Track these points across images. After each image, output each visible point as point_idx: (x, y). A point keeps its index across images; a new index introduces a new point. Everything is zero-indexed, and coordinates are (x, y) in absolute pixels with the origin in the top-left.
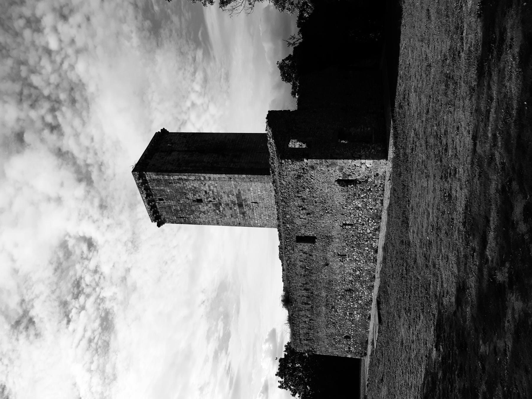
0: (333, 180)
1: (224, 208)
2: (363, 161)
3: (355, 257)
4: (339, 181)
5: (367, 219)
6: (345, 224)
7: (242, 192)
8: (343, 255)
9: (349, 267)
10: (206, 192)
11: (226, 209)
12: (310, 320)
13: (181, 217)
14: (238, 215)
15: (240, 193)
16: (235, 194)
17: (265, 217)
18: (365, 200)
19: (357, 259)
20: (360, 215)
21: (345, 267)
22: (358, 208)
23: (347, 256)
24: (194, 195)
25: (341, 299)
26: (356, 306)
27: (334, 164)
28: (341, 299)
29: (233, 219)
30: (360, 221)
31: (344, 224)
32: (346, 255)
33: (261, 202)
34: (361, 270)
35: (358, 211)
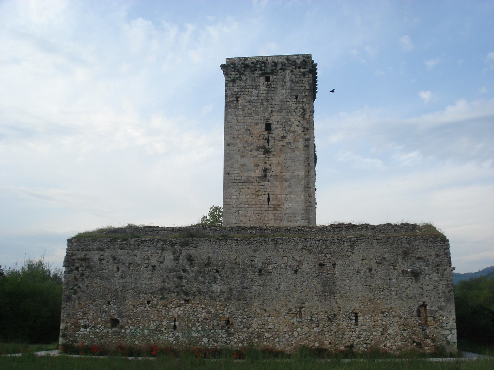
0: (426, 300)
1: (256, 157)
2: (455, 332)
3: (299, 330)
4: (424, 305)
5: (368, 342)
6: (357, 317)
7: (287, 183)
8: (300, 315)
9: (278, 322)
10: (284, 137)
11: (256, 159)
12: (154, 267)
13: (237, 98)
14: (246, 174)
15: (285, 180)
16: (282, 174)
17: (243, 209)
18: (399, 337)
19: (295, 334)
20: (374, 333)
21: (277, 317)
22: (385, 330)
23: (300, 320)
24: (278, 122)
25: (208, 313)
26: (194, 335)
27: (448, 300)
28: (208, 313)
29: (237, 166)
30: (364, 333)
31: (356, 314)
32: (301, 318)
33: (271, 206)
34: (274, 339)
35: (381, 330)
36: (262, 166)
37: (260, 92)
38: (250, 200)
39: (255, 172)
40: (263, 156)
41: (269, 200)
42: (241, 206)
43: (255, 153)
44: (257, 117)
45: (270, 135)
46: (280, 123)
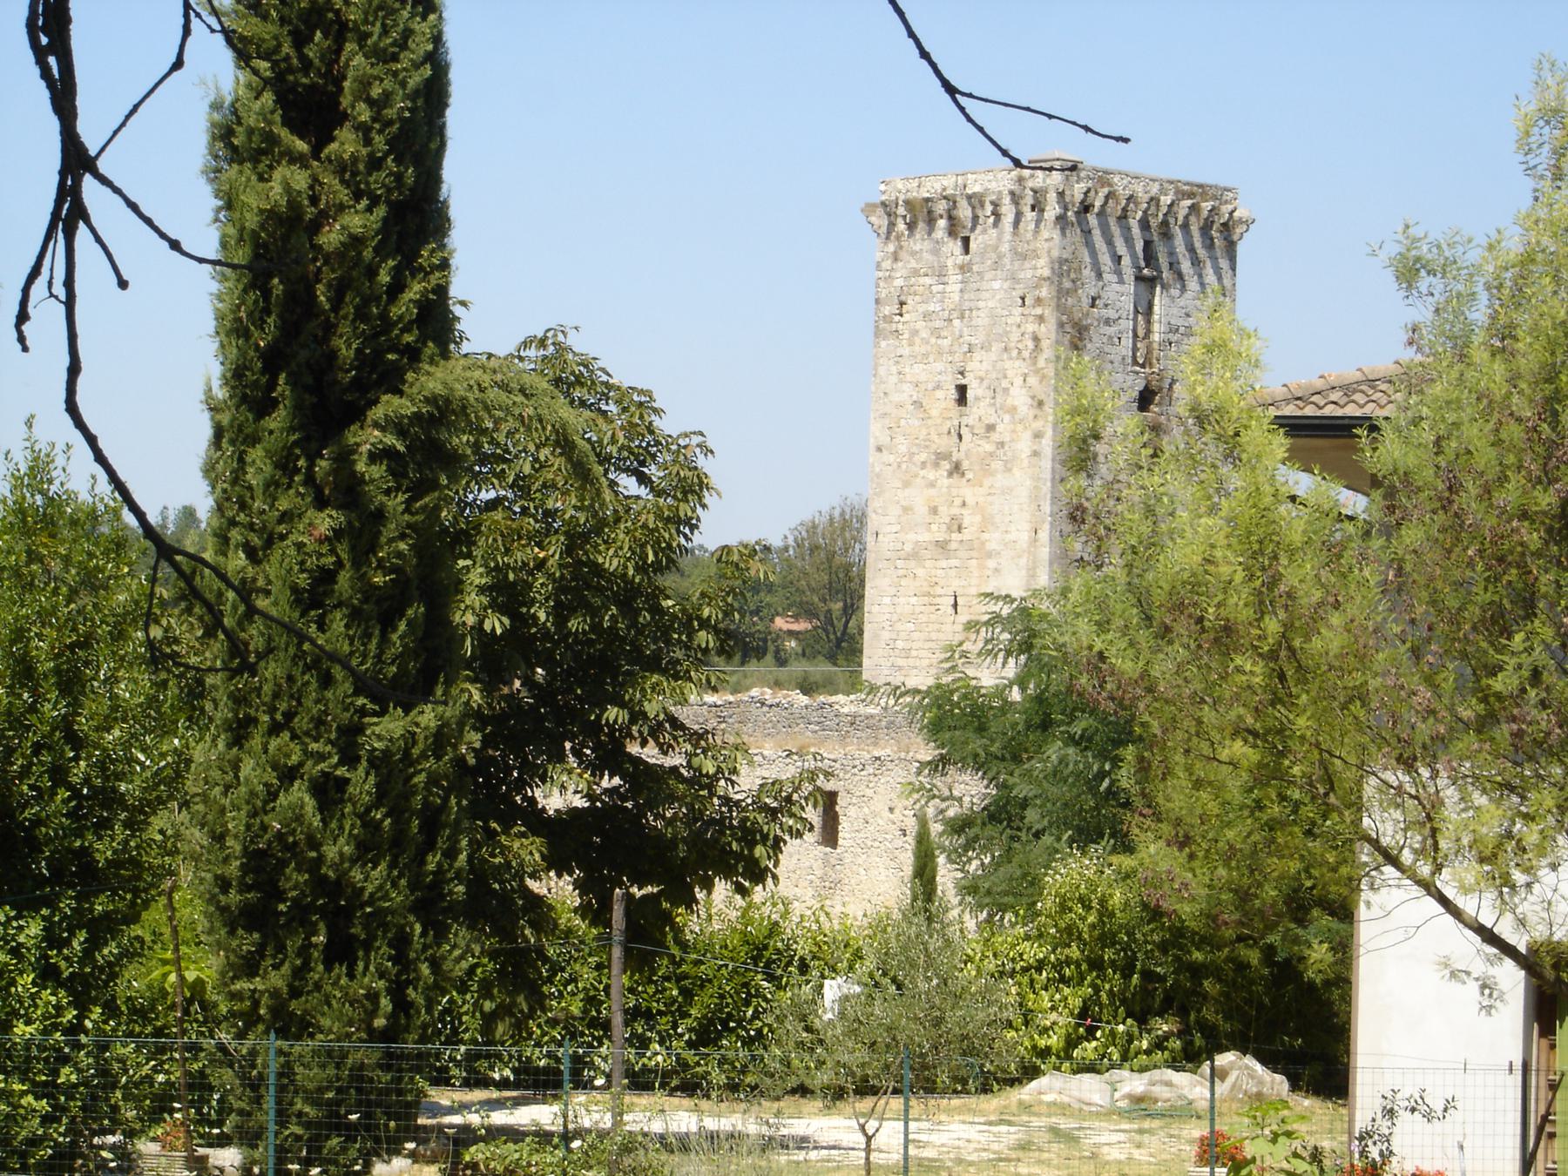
1: (932, 485)
7: (991, 563)
11: (932, 492)
15: (989, 555)
36: (945, 513)
37: (948, 289)
38: (918, 609)
39: (929, 530)
40: (946, 482)
41: (955, 605)
42: (899, 626)
43: (931, 474)
44: (939, 366)
45: (965, 421)
46: (986, 383)
